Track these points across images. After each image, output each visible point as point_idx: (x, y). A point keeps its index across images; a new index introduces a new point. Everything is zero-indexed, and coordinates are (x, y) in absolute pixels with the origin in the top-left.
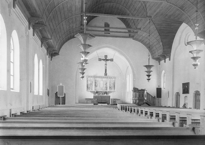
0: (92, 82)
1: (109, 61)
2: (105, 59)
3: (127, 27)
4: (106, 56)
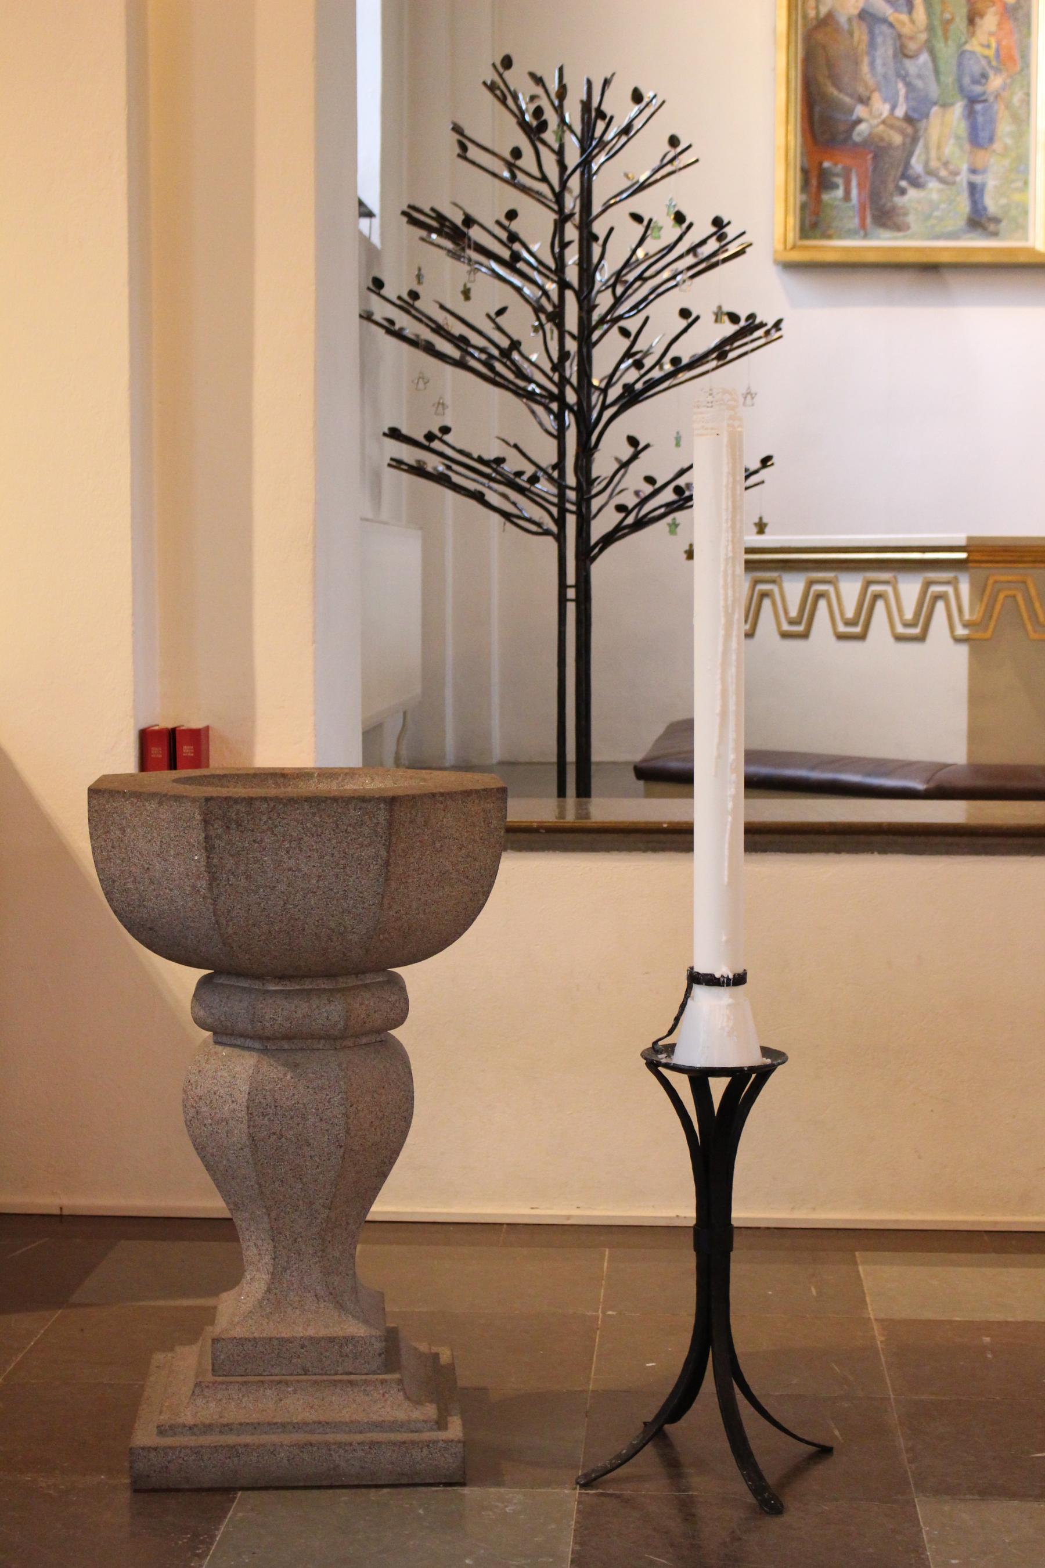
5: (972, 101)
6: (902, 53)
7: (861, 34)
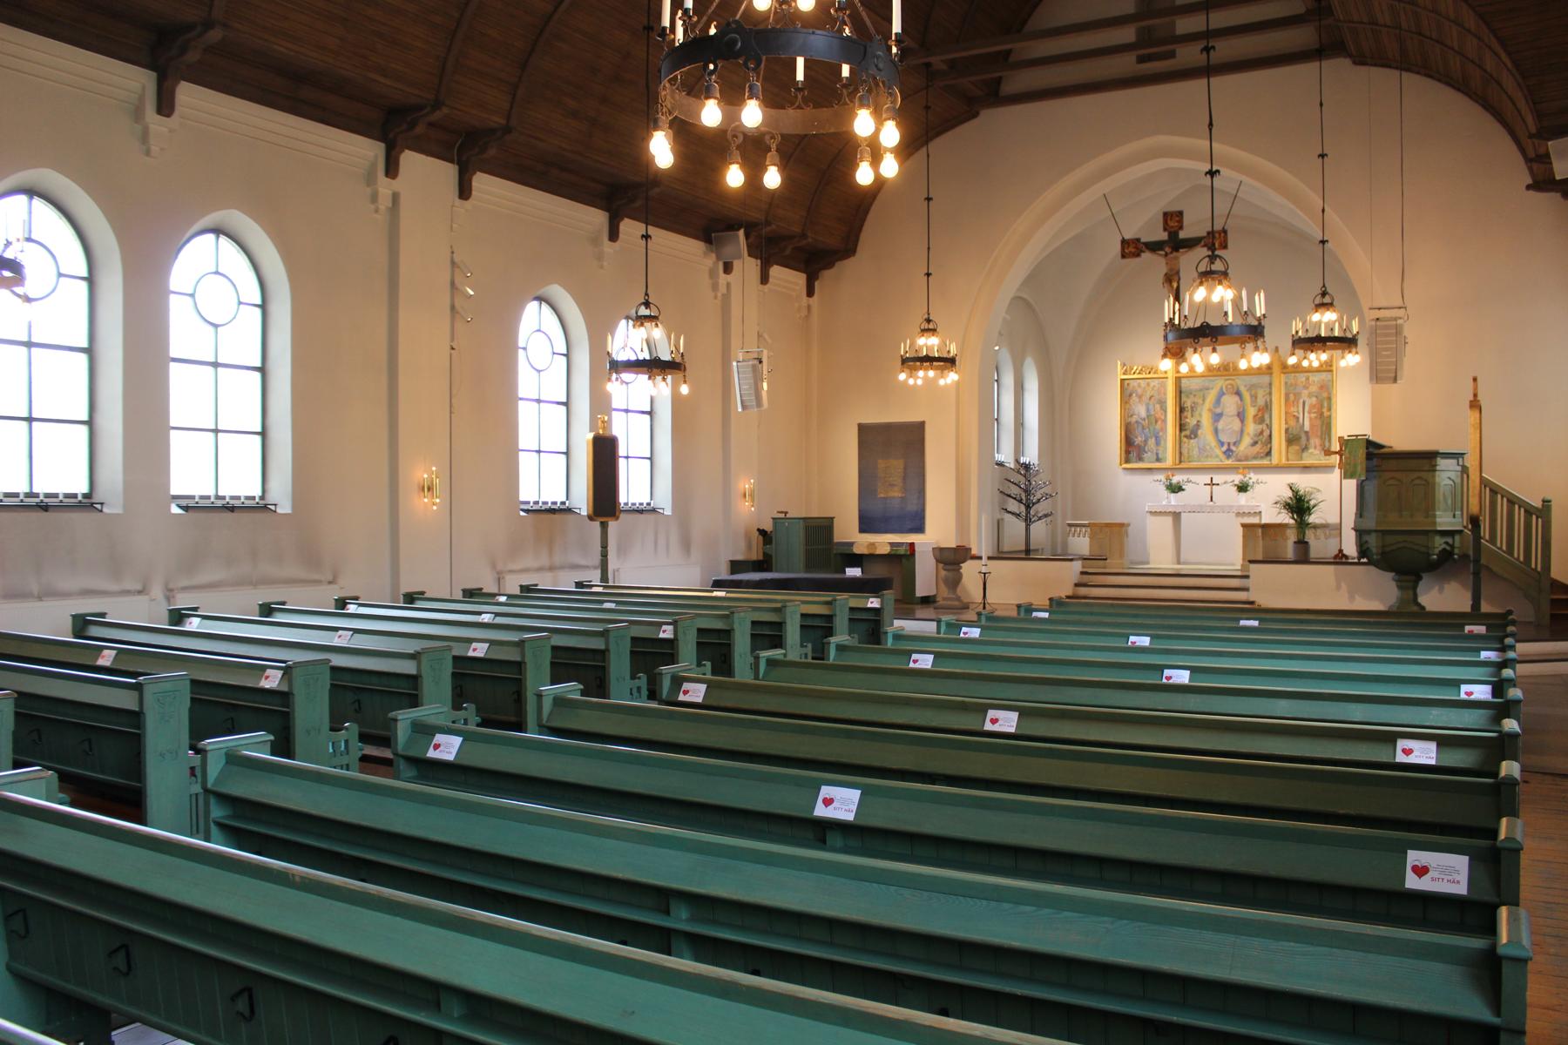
0: (1162, 403)
2: (1164, 236)
4: (1173, 219)
5: (1156, 437)
6: (1143, 428)
7: (1136, 425)
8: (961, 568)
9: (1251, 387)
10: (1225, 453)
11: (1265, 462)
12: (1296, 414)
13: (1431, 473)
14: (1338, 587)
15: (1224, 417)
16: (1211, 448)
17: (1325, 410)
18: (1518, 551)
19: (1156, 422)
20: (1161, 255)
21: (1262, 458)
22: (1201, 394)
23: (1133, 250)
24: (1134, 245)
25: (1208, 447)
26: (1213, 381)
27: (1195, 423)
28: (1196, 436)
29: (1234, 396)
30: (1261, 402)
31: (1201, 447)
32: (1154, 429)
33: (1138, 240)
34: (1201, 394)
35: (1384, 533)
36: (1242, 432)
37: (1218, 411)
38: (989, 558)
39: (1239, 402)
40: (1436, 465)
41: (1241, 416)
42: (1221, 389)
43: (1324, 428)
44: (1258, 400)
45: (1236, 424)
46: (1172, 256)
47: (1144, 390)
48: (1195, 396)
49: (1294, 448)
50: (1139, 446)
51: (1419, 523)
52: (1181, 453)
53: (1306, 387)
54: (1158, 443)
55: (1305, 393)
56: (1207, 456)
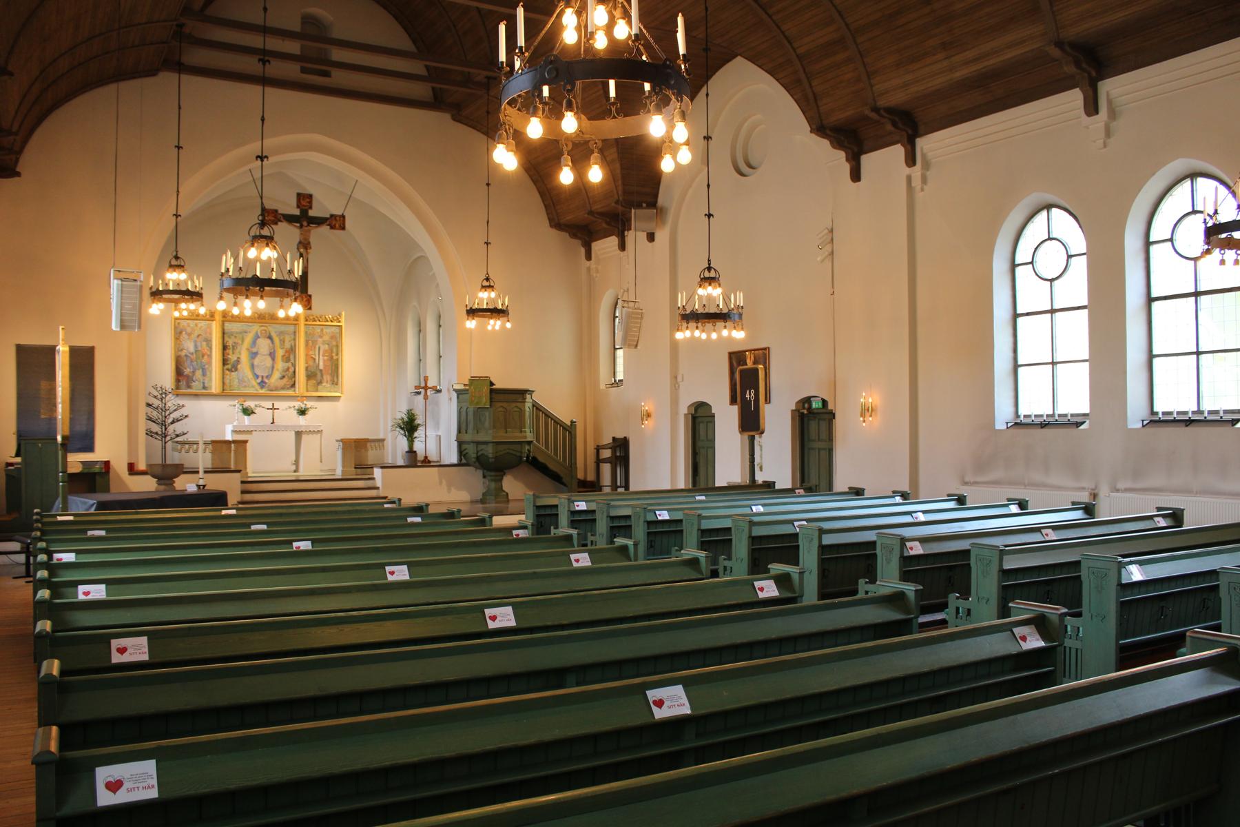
0: (208, 341)
1: (325, 229)
2: (297, 212)
3: (417, 48)
4: (305, 200)
5: (203, 369)
6: (192, 361)
8: (174, 482)
9: (281, 334)
10: (259, 384)
11: (291, 392)
12: (313, 356)
13: (523, 404)
14: (441, 483)
15: (259, 356)
16: (249, 380)
17: (334, 355)
18: (559, 453)
19: (203, 356)
20: (295, 226)
21: (288, 389)
22: (241, 336)
23: (273, 218)
24: (273, 215)
25: (246, 379)
26: (250, 326)
27: (235, 359)
28: (236, 370)
29: (266, 339)
30: (287, 345)
31: (240, 378)
32: (201, 362)
33: (276, 211)
34: (241, 336)
35: (498, 443)
36: (273, 367)
37: (254, 350)
38: (206, 472)
39: (271, 345)
40: (525, 399)
41: (272, 355)
42: (257, 333)
43: (334, 367)
44: (286, 344)
45: (269, 362)
46: (306, 228)
47: (193, 330)
48: (235, 337)
49: (313, 382)
50: (188, 376)
51: (514, 436)
52: (224, 383)
53: (321, 337)
54: (204, 374)
55: (320, 340)
56: (245, 386)
